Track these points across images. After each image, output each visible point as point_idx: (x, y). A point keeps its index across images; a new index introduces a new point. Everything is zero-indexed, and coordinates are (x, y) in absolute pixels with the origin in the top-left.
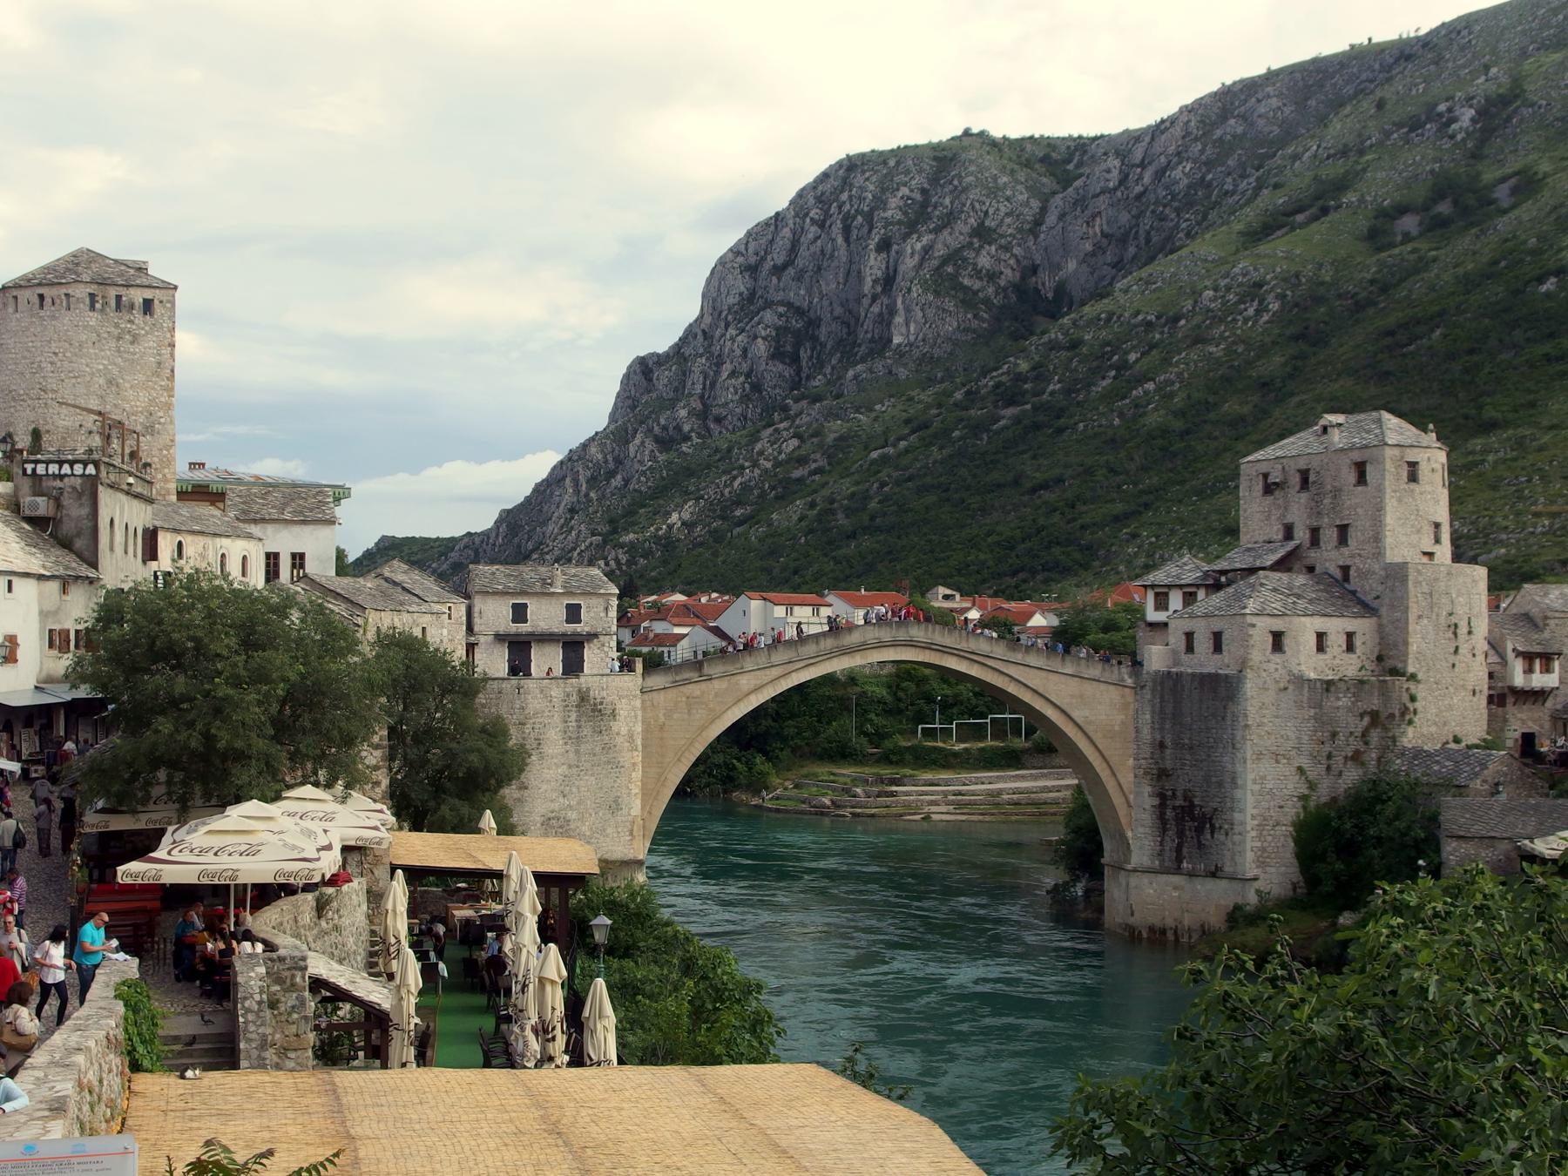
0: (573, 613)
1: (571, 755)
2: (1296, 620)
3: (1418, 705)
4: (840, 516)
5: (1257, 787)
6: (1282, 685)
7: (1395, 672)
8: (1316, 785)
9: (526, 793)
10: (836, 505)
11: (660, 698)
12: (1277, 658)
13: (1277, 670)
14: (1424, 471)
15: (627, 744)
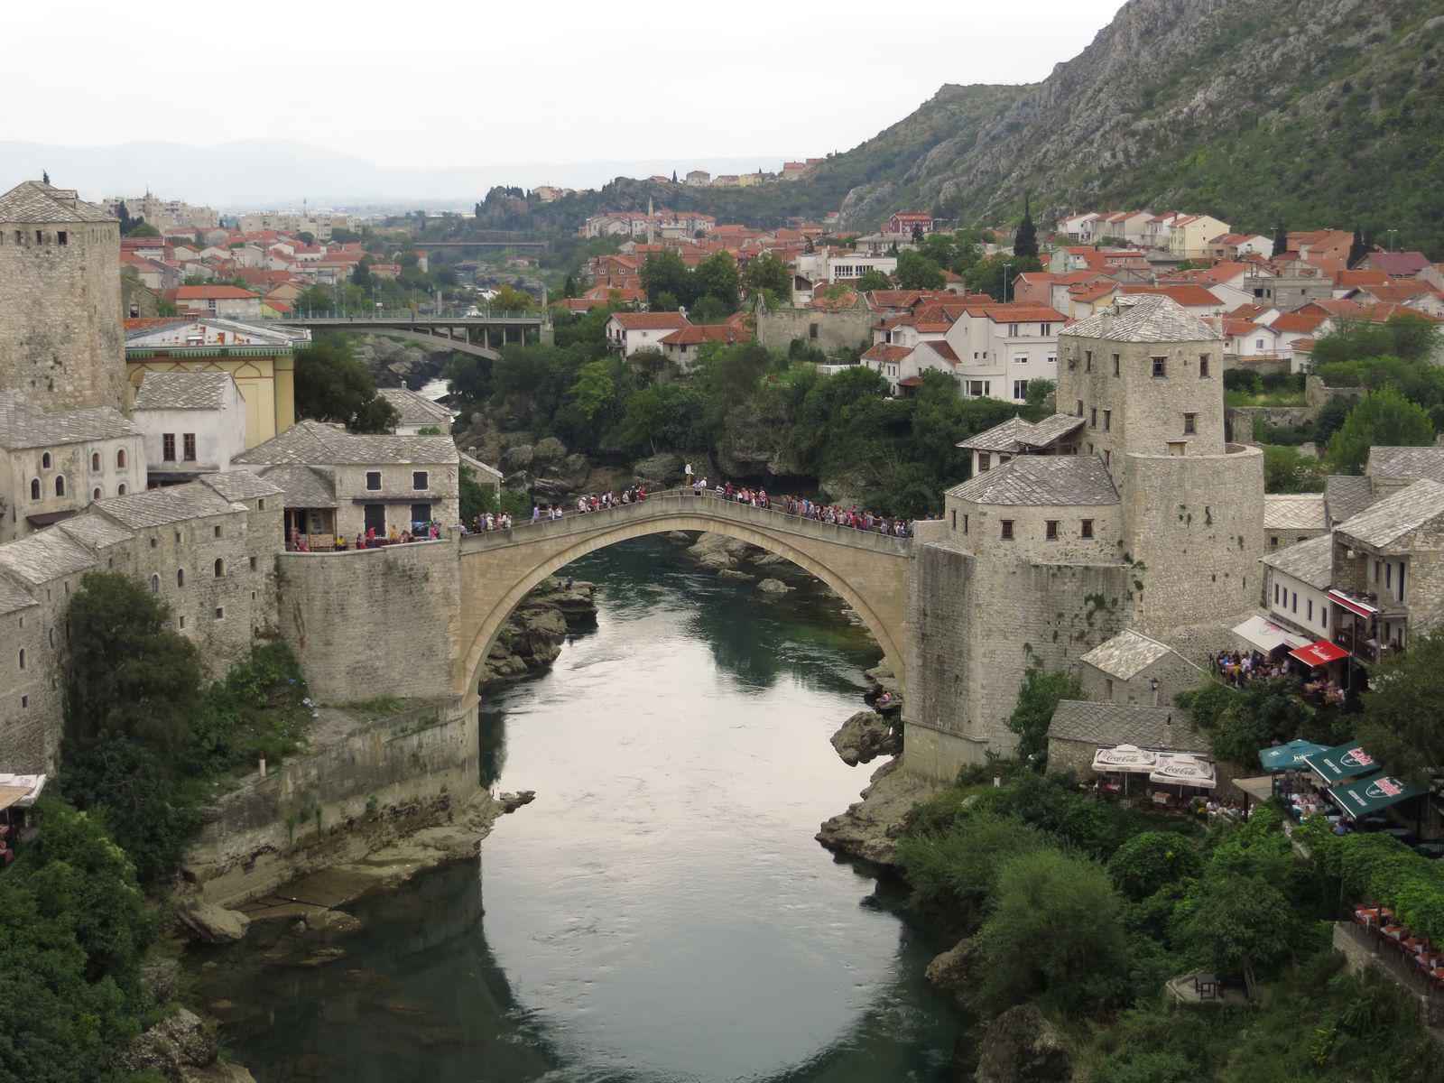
0: (420, 480)
1: (377, 614)
2: (1026, 509)
3: (1145, 591)
4: (1375, 104)
5: (987, 660)
6: (1011, 570)
7: (1127, 558)
8: (1042, 661)
9: (330, 648)
10: (1373, 90)
11: (476, 560)
12: (1007, 544)
13: (1006, 555)
14: (1173, 365)
15: (441, 601)
